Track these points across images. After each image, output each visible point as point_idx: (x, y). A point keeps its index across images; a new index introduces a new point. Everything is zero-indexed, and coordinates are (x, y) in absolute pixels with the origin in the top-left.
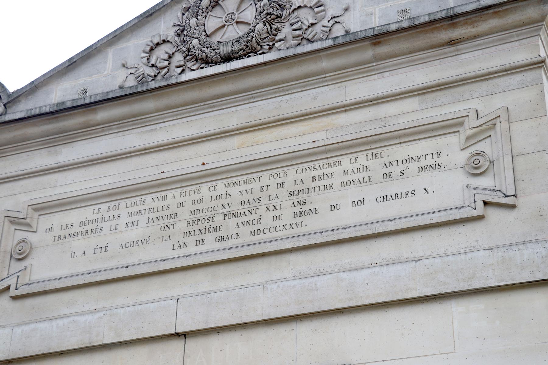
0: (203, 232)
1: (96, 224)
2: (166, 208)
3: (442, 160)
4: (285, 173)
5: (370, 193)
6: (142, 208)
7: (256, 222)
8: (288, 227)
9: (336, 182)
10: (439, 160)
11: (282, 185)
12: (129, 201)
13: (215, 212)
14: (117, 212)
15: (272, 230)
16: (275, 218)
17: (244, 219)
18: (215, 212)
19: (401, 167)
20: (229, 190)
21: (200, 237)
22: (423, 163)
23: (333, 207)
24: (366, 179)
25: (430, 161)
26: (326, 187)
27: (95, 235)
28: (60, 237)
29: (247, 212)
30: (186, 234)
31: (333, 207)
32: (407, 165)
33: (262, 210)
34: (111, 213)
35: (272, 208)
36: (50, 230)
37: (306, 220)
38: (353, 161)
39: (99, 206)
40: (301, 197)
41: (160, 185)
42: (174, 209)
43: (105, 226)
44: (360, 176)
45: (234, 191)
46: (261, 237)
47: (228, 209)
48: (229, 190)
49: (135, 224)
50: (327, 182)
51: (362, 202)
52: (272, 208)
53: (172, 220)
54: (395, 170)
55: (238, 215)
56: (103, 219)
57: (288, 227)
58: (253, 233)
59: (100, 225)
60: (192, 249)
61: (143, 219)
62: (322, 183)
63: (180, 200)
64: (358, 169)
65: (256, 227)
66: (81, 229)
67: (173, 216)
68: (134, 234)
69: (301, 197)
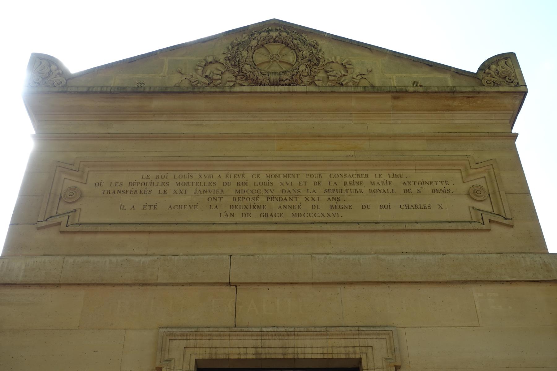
0: (248, 207)
1: (145, 186)
2: (212, 184)
4: (320, 176)
6: (190, 180)
7: (297, 207)
8: (326, 215)
10: (447, 187)
11: (319, 183)
12: (177, 174)
13: (259, 194)
14: (165, 180)
15: (311, 215)
16: (313, 207)
17: (286, 203)
18: (259, 194)
19: (418, 187)
20: (271, 180)
21: (246, 211)
22: (435, 187)
23: (364, 207)
24: (390, 191)
25: (439, 186)
26: (356, 191)
27: (144, 195)
28: (109, 192)
29: (288, 199)
30: (232, 207)
31: (364, 207)
32: (422, 186)
33: (301, 199)
34: (160, 181)
35: (310, 199)
36: (100, 184)
38: (378, 176)
39: (148, 173)
40: (336, 195)
44: (385, 188)
46: (302, 219)
47: (270, 194)
48: (271, 180)
49: (183, 192)
50: (358, 187)
51: (389, 206)
52: (310, 199)
53: (218, 194)
54: (414, 188)
55: (280, 200)
56: (152, 184)
57: (326, 215)
58: (295, 215)
59: (149, 188)
60: (239, 219)
62: (353, 187)
63: (227, 180)
64: (383, 183)
65: (297, 211)
66: (130, 188)
67: (220, 192)
68: (182, 199)
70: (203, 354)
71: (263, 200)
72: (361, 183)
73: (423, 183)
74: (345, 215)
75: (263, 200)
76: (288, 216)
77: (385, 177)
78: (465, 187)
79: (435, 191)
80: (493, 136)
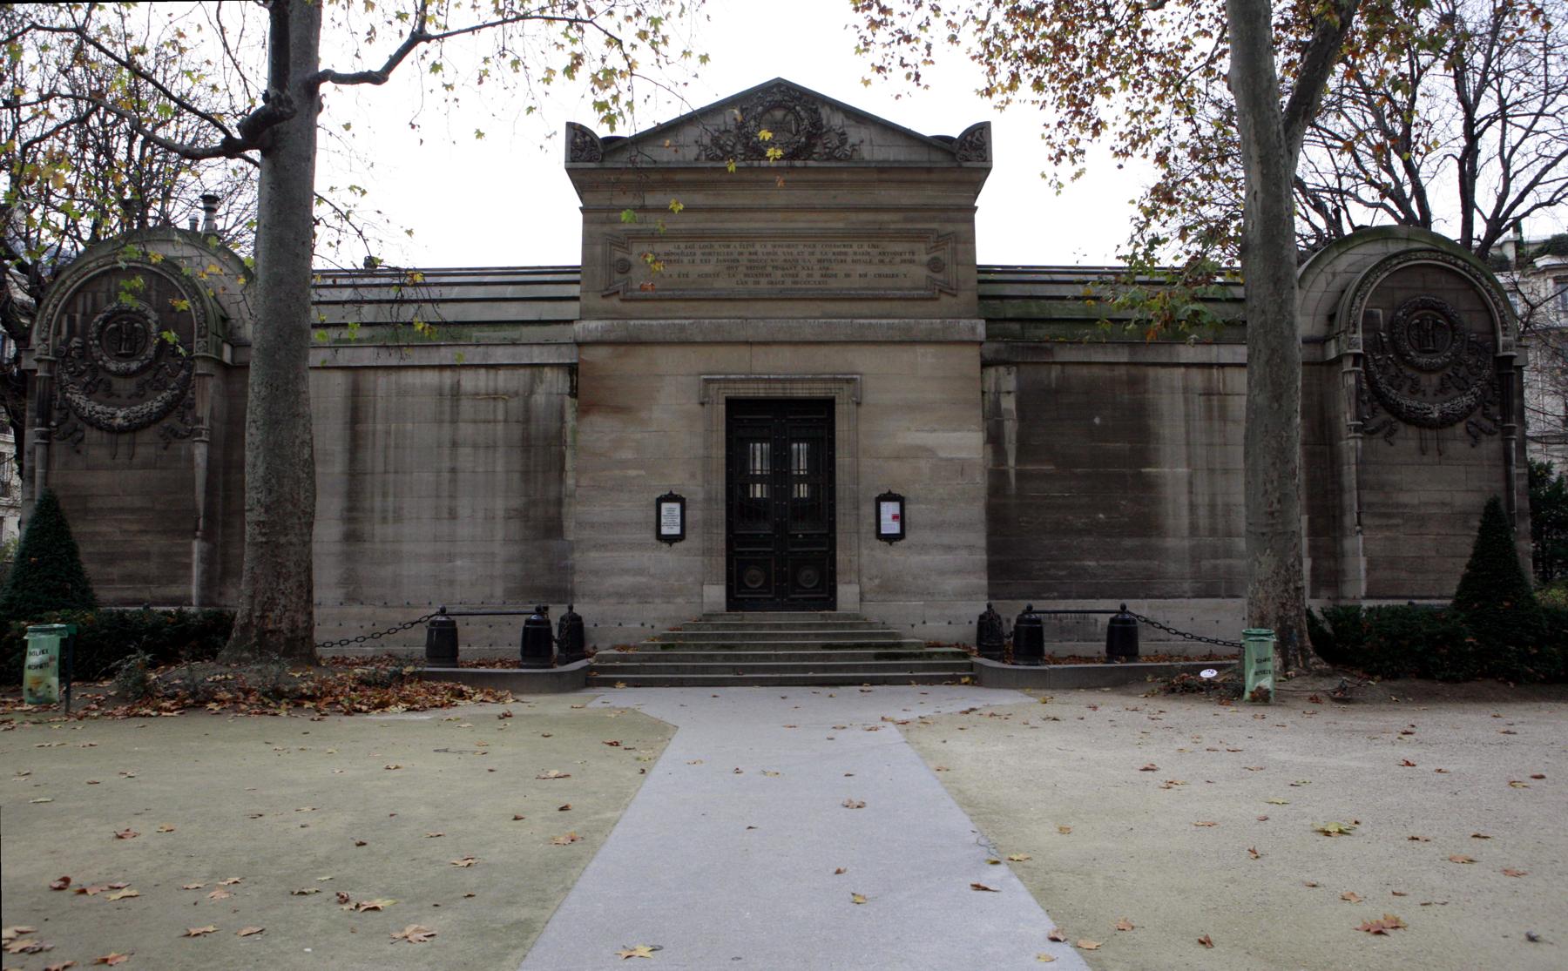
3: (916, 258)
5: (872, 270)
9: (849, 259)
23: (848, 275)
25: (907, 257)
31: (848, 275)
37: (830, 280)
40: (826, 264)
41: (726, 237)
42: (735, 256)
43: (686, 259)
45: (779, 251)
61: (714, 259)
68: (708, 269)
69: (826, 264)
70: (732, 394)
71: (769, 269)
72: (845, 254)
73: (895, 254)
74: (833, 284)
75: (769, 269)
76: (789, 283)
77: (866, 248)
78: (926, 258)
79: (903, 261)
80: (959, 209)
